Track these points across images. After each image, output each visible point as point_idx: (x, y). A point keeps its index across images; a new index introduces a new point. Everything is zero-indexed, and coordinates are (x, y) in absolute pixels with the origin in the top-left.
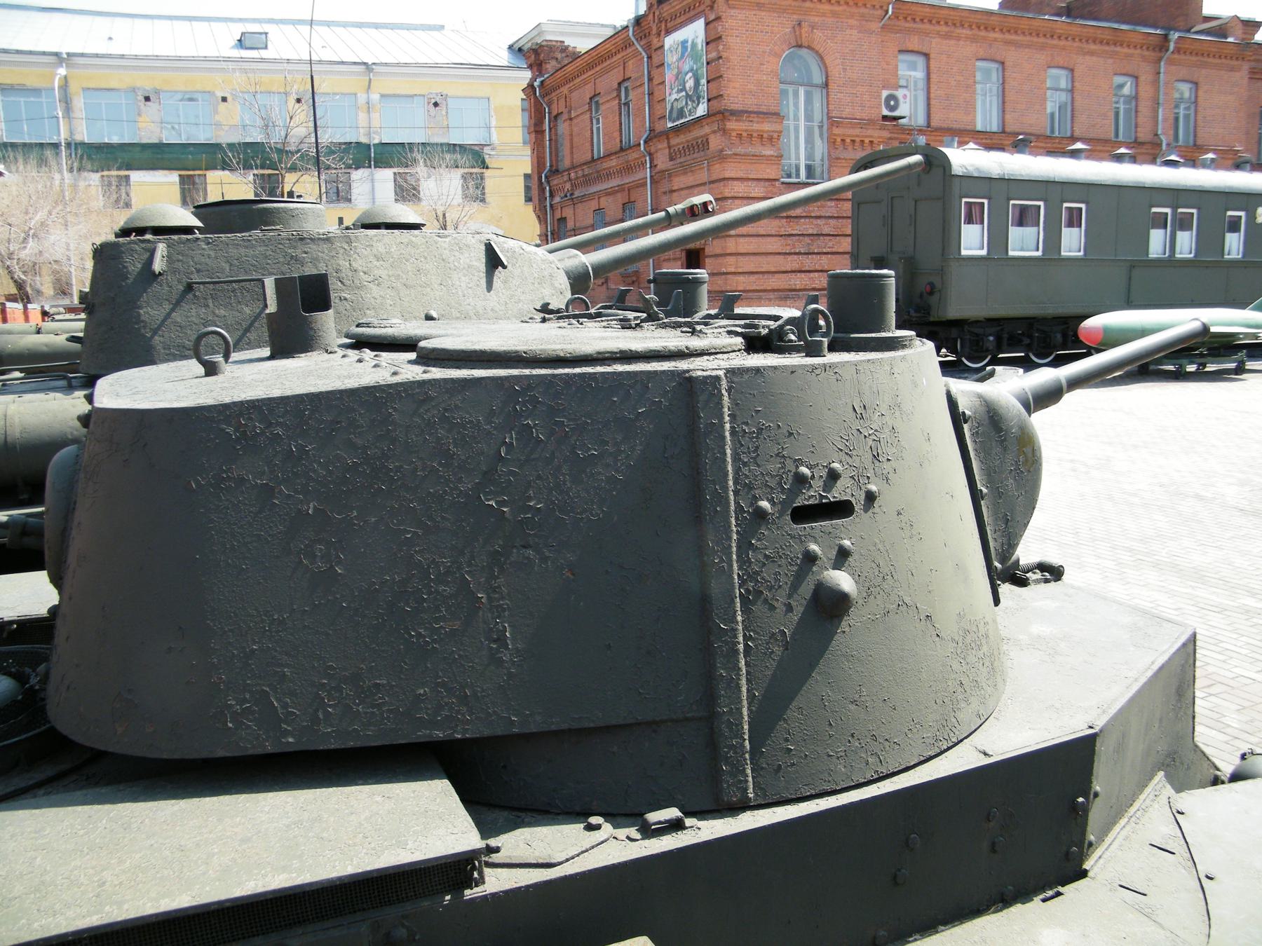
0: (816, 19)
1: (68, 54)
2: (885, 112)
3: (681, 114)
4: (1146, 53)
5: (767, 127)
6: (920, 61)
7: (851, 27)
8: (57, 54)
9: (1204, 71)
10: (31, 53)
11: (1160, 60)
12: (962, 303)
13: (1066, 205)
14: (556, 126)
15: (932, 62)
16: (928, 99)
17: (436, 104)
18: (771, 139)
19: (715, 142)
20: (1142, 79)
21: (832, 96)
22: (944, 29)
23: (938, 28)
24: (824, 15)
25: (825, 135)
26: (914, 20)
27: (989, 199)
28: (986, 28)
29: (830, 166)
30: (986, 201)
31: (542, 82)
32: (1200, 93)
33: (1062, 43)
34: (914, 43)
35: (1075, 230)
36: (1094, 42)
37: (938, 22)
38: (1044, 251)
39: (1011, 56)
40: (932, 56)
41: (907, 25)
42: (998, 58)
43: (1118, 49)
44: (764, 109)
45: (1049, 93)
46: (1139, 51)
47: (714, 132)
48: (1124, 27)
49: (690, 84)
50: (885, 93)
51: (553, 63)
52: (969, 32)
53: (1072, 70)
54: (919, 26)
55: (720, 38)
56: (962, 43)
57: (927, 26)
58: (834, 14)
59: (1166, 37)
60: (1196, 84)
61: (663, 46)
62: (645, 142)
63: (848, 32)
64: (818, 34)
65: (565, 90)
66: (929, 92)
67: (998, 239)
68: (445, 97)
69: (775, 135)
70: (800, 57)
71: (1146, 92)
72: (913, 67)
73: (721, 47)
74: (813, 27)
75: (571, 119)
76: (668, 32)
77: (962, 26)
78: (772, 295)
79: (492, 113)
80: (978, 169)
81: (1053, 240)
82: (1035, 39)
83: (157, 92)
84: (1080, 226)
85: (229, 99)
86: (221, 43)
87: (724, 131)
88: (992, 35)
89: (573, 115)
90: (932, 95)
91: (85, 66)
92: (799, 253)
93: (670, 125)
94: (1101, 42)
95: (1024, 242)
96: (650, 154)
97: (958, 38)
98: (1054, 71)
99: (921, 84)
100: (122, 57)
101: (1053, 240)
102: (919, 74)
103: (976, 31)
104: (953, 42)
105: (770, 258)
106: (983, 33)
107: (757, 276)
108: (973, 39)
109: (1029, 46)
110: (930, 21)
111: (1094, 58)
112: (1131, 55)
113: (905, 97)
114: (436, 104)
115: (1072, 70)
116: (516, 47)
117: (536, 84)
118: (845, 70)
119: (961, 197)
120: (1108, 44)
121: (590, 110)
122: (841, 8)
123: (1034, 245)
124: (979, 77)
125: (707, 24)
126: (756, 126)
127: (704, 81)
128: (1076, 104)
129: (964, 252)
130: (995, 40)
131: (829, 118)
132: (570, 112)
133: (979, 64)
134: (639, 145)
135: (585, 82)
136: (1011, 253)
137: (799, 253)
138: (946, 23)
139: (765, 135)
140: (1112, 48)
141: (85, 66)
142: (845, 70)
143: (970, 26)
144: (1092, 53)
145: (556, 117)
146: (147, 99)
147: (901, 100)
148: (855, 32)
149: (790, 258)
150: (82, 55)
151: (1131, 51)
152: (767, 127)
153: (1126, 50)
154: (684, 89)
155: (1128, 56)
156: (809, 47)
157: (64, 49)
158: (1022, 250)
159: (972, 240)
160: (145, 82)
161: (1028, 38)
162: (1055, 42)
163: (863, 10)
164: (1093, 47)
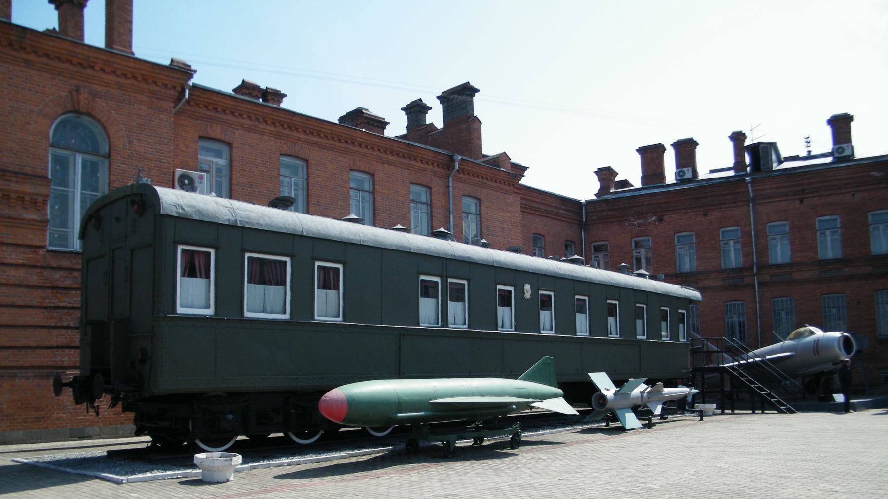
0: (100, 88)
4: (436, 169)
5: (28, 188)
6: (225, 149)
9: (485, 191)
11: (449, 176)
12: (170, 378)
13: (317, 263)
15: (234, 150)
16: (231, 185)
18: (34, 202)
20: (435, 189)
22: (247, 122)
23: (241, 121)
26: (216, 109)
27: (216, 248)
28: (289, 127)
30: (212, 252)
32: (483, 207)
33: (363, 150)
34: (216, 131)
35: (332, 293)
36: (391, 153)
37: (241, 115)
38: (291, 314)
39: (315, 155)
40: (234, 145)
41: (208, 113)
42: (302, 156)
43: (413, 163)
44: (28, 170)
45: (352, 192)
46: (431, 167)
48: (417, 144)
50: (179, 171)
52: (272, 129)
53: (373, 175)
54: (223, 116)
56: (266, 137)
57: (230, 117)
59: (452, 159)
60: (479, 200)
64: (100, 103)
66: (231, 179)
67: (229, 297)
69: (41, 199)
71: (438, 201)
72: (219, 155)
74: (94, 95)
77: (266, 122)
78: (30, 373)
80: (199, 211)
81: (303, 302)
82: (338, 144)
84: (337, 288)
88: (295, 134)
90: (234, 182)
92: (68, 328)
94: (398, 155)
95: (264, 303)
97: (262, 133)
98: (358, 175)
99: (226, 172)
101: (303, 302)
102: (222, 162)
103: (280, 129)
104: (256, 136)
105: (30, 332)
106: (287, 132)
107: (11, 351)
108: (278, 136)
109: (332, 149)
110: (232, 113)
111: (393, 168)
112: (425, 169)
113: (201, 177)
115: (373, 175)
119: (176, 243)
120: (403, 157)
122: (129, 82)
123: (279, 307)
124: (283, 171)
126: (14, 187)
128: (377, 204)
129: (180, 310)
130: (299, 139)
133: (284, 159)
136: (247, 314)
137: (68, 328)
138: (249, 117)
139: (27, 198)
140: (408, 161)
142: (130, 142)
143: (274, 123)
144: (390, 163)
147: (197, 180)
149: (55, 332)
151: (425, 166)
152: (28, 188)
153: (419, 164)
156: (88, 114)
158: (264, 311)
159: (193, 297)
161: (331, 142)
162: (356, 149)
163: (153, 87)
164: (390, 157)
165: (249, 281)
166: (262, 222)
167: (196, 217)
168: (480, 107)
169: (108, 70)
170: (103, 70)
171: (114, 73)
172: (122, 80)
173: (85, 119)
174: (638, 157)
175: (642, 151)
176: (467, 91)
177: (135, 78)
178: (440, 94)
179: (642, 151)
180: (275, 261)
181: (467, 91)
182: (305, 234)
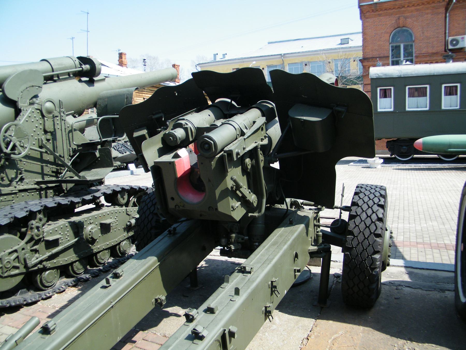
0: (408, 14)
1: (284, 54)
2: (450, 47)
7: (427, 14)
8: (281, 55)
10: (268, 56)
24: (412, 11)
44: (382, 55)
50: (450, 39)
58: (417, 10)
63: (425, 16)
64: (409, 20)
67: (400, 103)
70: (405, 30)
74: (406, 18)
80: (385, 75)
83: (309, 62)
85: (304, 65)
86: (334, 43)
91: (289, 57)
100: (299, 53)
118: (423, 33)
122: (421, 7)
141: (289, 57)
142: (423, 33)
146: (306, 65)
147: (460, 40)
148: (429, 16)
150: (288, 54)
157: (282, 53)
159: (385, 105)
160: (305, 59)
163: (433, 5)
165: (409, 97)
166: (413, 73)
167: (384, 77)
169: (411, 5)
170: (408, 6)
171: (413, 5)
172: (418, 7)
173: (404, 28)
177: (423, 4)
180: (420, 88)
182: (435, 74)
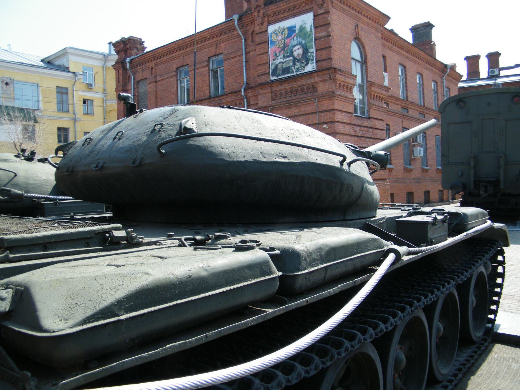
3: (287, 70)
14: (138, 87)
17: (7, 84)
19: (322, 88)
21: (369, 70)
25: (365, 91)
29: (369, 108)
31: (131, 60)
47: (324, 81)
49: (298, 51)
51: (135, 50)
55: (329, 24)
61: (266, 31)
62: (245, 90)
65: (152, 64)
68: (13, 81)
73: (330, 29)
75: (156, 82)
76: (270, 23)
79: (40, 92)
87: (334, 80)
89: (158, 79)
93: (273, 78)
96: (247, 98)
114: (7, 84)
116: (47, 60)
117: (128, 60)
121: (176, 75)
125: (315, 16)
127: (313, 50)
131: (367, 81)
132: (156, 77)
134: (241, 91)
135: (173, 59)
145: (138, 82)
148: (374, 36)
154: (292, 55)
155: (435, 72)
168: (436, 36)
174: (465, 63)
175: (467, 59)
176: (429, 26)
178: (411, 28)
179: (467, 59)
181: (429, 26)
